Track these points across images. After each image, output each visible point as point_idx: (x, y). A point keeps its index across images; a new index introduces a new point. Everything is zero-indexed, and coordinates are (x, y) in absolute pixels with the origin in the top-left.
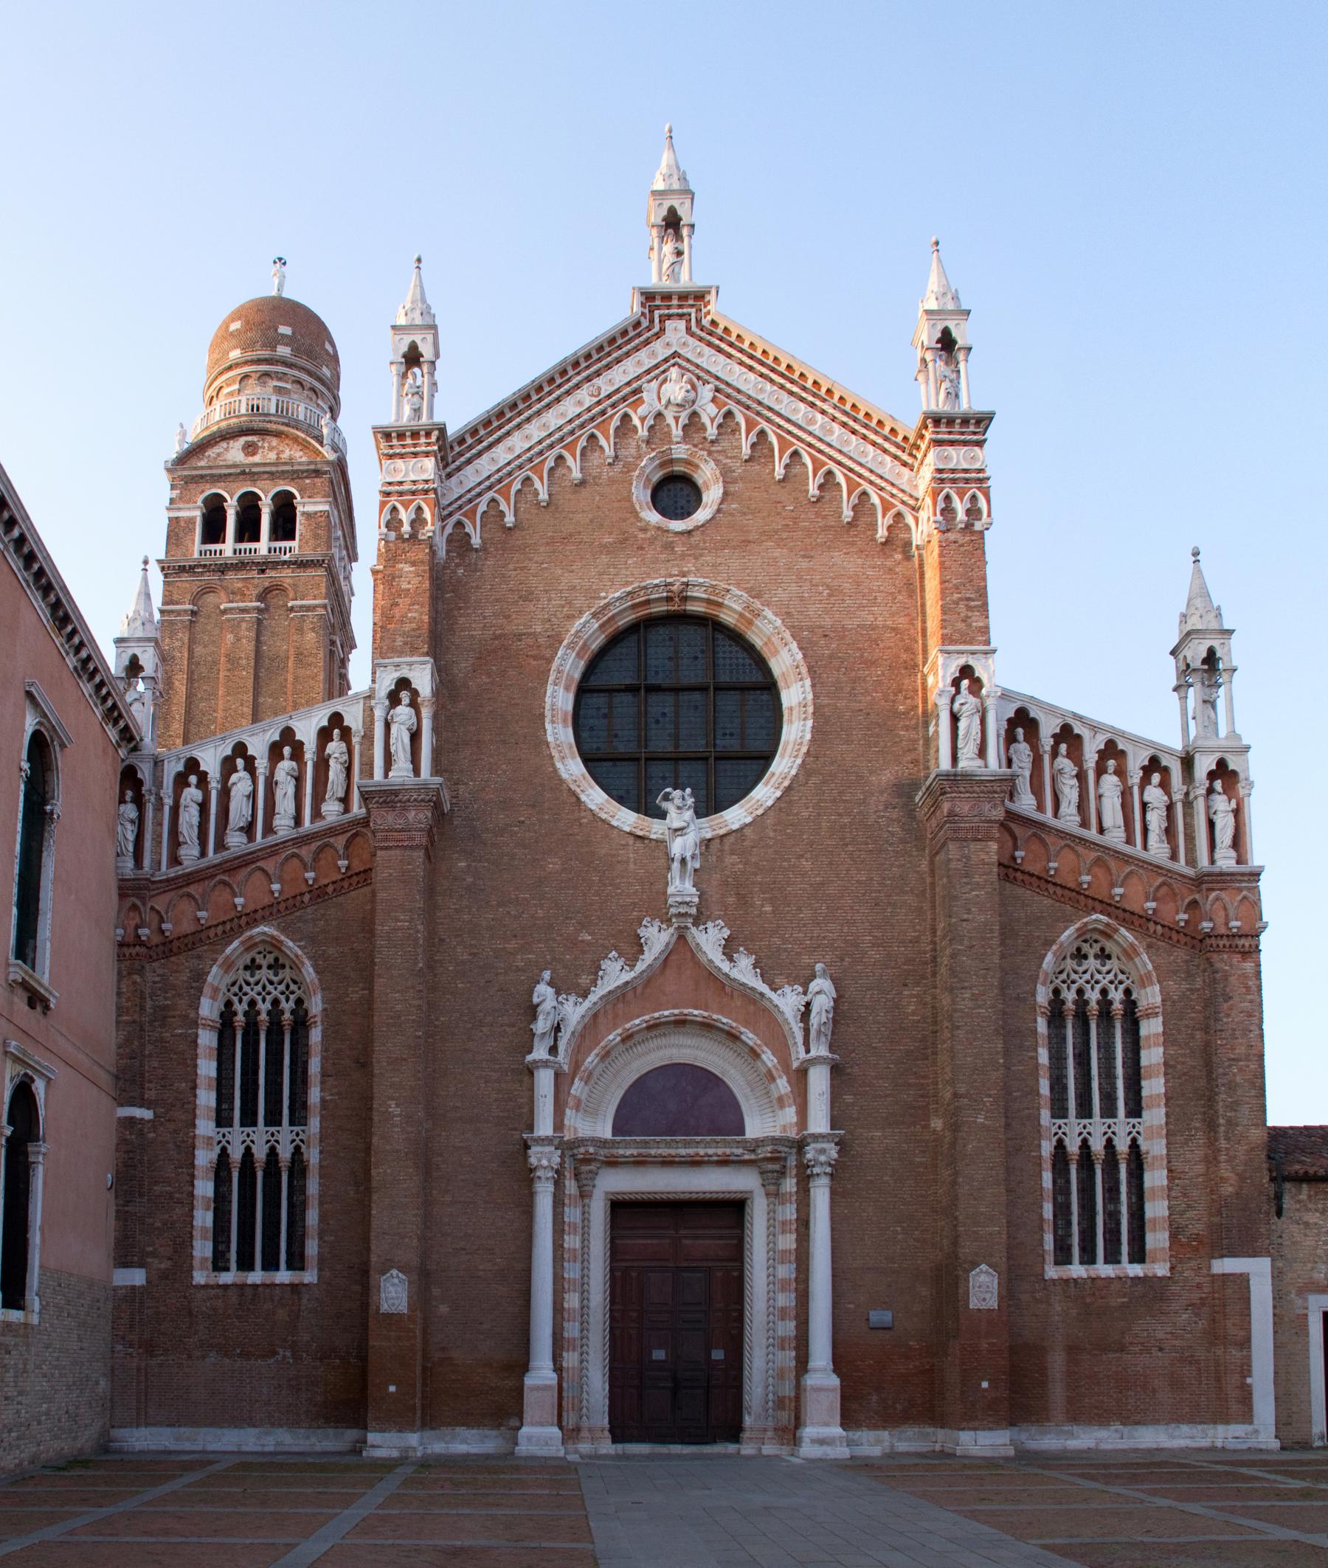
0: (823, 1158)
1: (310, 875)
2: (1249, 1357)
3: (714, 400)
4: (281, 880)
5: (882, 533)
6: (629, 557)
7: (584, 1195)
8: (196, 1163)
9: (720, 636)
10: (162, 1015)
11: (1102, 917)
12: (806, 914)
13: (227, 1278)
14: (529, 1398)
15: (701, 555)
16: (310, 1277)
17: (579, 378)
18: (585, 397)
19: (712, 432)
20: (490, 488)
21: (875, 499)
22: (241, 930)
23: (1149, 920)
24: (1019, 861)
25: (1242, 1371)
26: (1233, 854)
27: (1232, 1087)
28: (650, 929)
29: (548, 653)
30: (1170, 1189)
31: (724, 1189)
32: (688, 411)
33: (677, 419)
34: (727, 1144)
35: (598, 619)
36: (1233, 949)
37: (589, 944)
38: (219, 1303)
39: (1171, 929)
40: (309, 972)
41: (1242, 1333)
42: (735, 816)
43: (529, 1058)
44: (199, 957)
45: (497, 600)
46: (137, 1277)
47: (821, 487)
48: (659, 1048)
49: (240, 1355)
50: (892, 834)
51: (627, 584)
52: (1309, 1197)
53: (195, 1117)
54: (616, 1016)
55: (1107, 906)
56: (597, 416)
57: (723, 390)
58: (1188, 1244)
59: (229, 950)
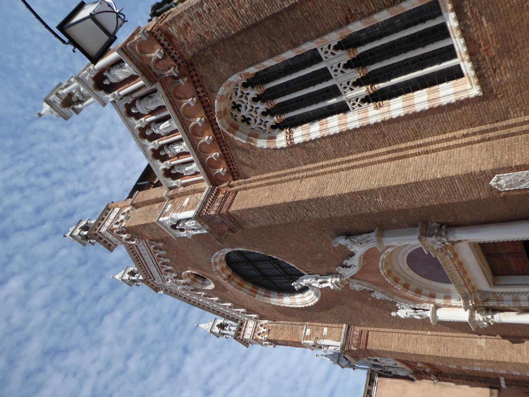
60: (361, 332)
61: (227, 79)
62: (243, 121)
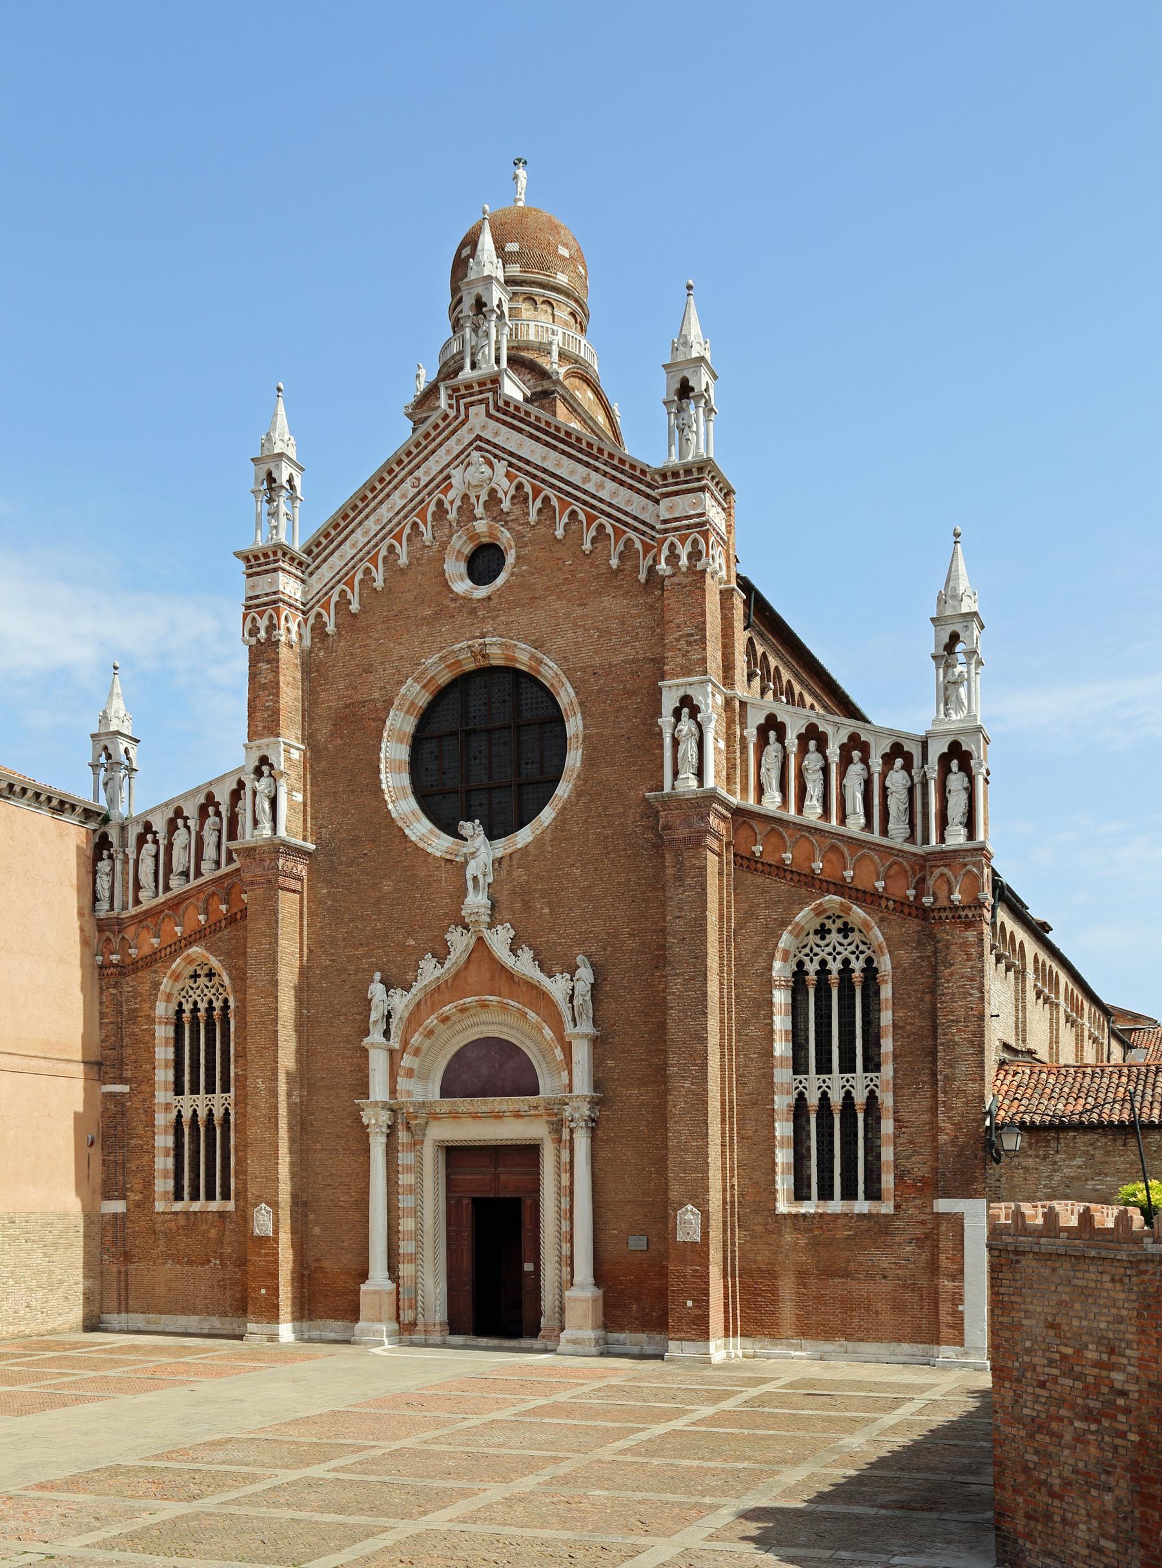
2: (961, 1288)
4: (206, 912)
5: (642, 577)
6: (443, 625)
7: (416, 1144)
10: (133, 1016)
11: (835, 897)
12: (576, 912)
13: (178, 1206)
15: (498, 616)
16: (230, 1206)
17: (403, 474)
19: (506, 505)
20: (339, 581)
27: (951, 1046)
29: (382, 715)
30: (896, 1137)
31: (520, 1137)
32: (487, 489)
33: (478, 497)
37: (414, 947)
38: (173, 1225)
42: (524, 836)
43: (366, 1041)
44: (156, 972)
45: (347, 675)
46: (117, 1207)
47: (594, 540)
49: (187, 1263)
50: (647, 840)
51: (442, 648)
55: (840, 888)
56: (416, 506)
58: (914, 1186)
59: (174, 966)
60: (299, 879)
61: (890, 952)
62: (823, 925)
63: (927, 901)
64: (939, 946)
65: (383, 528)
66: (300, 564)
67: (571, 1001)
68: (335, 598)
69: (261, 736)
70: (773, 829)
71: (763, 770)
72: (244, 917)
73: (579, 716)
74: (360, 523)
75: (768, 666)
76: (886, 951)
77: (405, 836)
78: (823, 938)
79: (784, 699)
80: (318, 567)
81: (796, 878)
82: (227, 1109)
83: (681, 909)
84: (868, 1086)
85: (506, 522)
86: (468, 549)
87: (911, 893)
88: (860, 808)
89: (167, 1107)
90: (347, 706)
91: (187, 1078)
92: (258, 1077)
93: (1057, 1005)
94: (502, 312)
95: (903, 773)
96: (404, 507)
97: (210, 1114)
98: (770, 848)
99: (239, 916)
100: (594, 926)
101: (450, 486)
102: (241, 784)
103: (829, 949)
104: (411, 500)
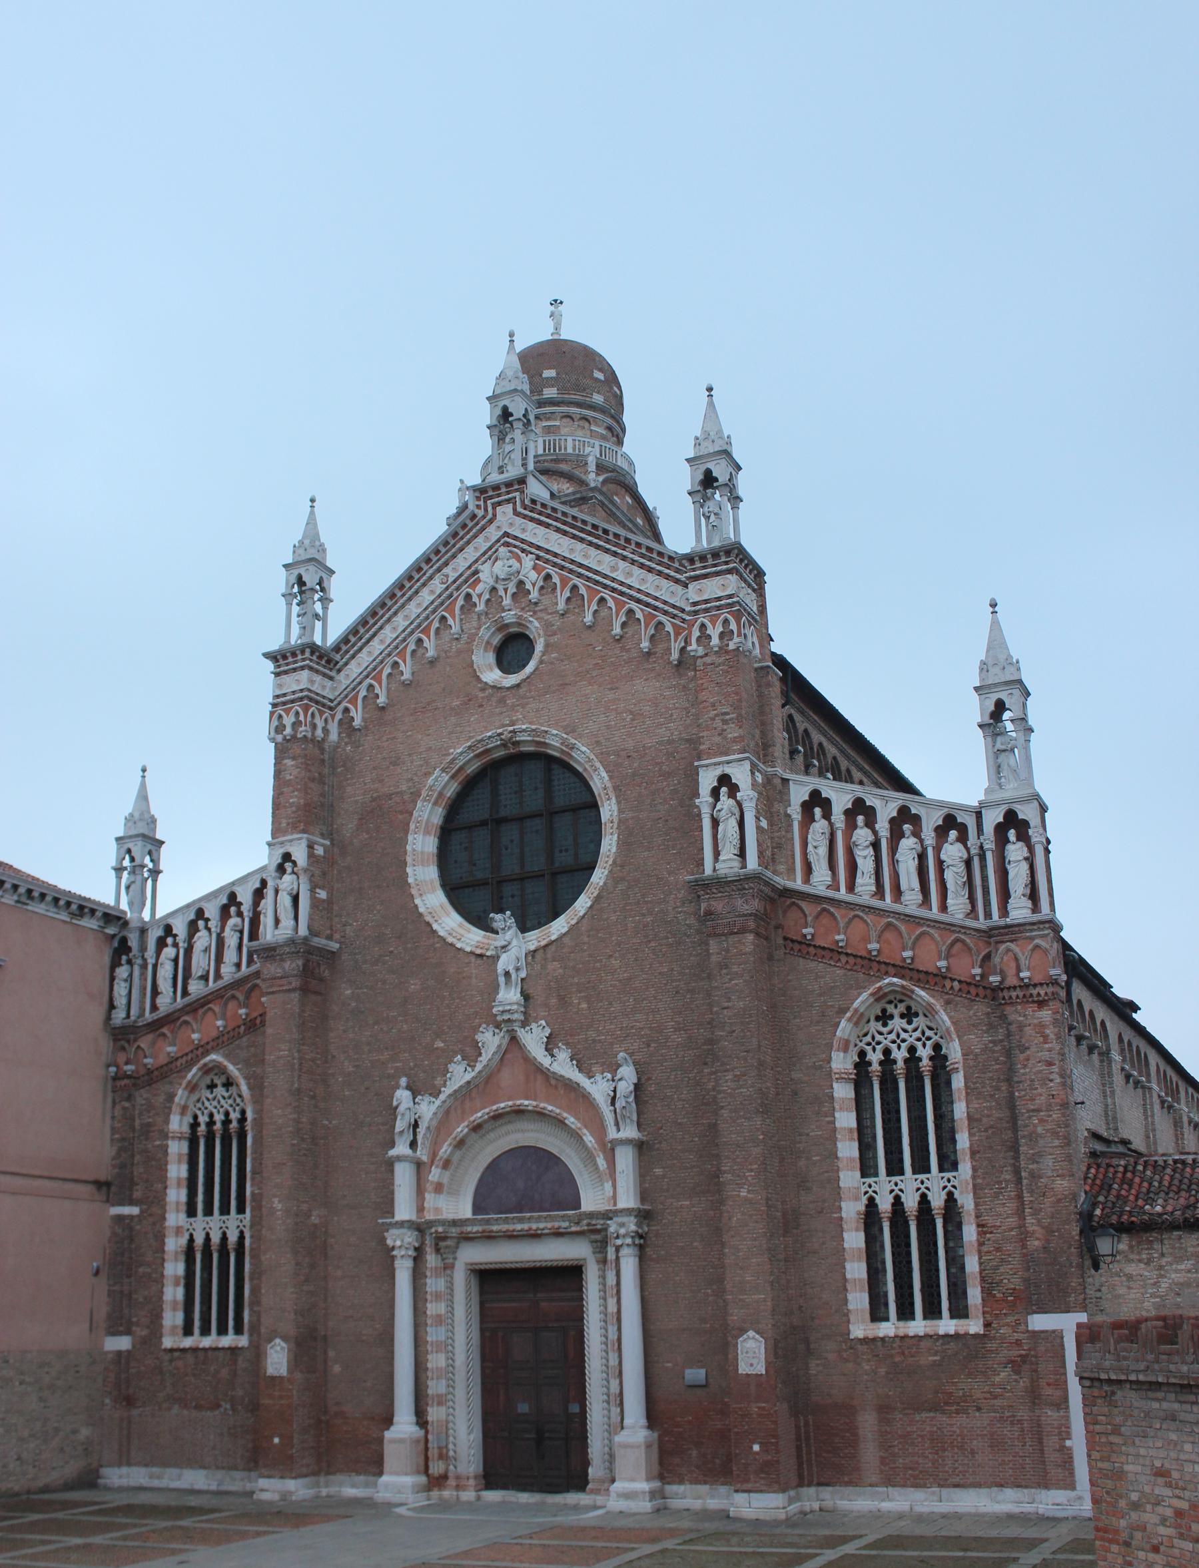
0: (622, 1231)
1: (242, 1011)
3: (535, 568)
5: (675, 655)
8: (166, 1249)
9: (555, 767)
11: (895, 980)
13: (188, 1342)
14: (388, 1449)
16: (243, 1341)
17: (431, 571)
18: (437, 585)
19: (534, 595)
20: (367, 677)
21: (669, 628)
22: (198, 1058)
23: (945, 978)
24: (809, 937)
25: (1060, 1434)
26: (1029, 904)
27: (1033, 1137)
28: (486, 1034)
30: (981, 1244)
32: (515, 581)
33: (506, 590)
34: (553, 1219)
35: (447, 773)
36: (1027, 1000)
37: (442, 1050)
39: (969, 984)
40: (244, 1088)
41: (1058, 1393)
42: (559, 926)
43: (392, 1153)
44: (171, 1083)
45: (374, 768)
46: (123, 1343)
47: (624, 625)
48: (508, 1133)
50: (689, 926)
52: (1131, 1247)
53: (165, 1212)
54: (463, 1112)
55: (901, 970)
56: (445, 601)
57: (543, 555)
59: (189, 1076)
62: (884, 1011)
63: (994, 979)
64: (1013, 1028)
65: (411, 623)
66: (329, 661)
67: (613, 1103)
68: (363, 693)
69: (285, 833)
70: (824, 910)
71: (810, 848)
72: (263, 1023)
73: (614, 800)
74: (389, 620)
75: (811, 743)
76: (954, 1036)
77: (435, 932)
78: (885, 1025)
79: (829, 775)
80: (346, 664)
81: (852, 960)
82: (242, 1232)
83: (729, 999)
84: (945, 1187)
85: (535, 612)
86: (496, 640)
87: (977, 971)
88: (916, 884)
89: (178, 1231)
90: (374, 800)
91: (200, 1198)
92: (275, 1196)
93: (1150, 1089)
94: (529, 420)
95: (959, 846)
96: (432, 603)
97: (224, 1238)
98: (822, 930)
99: (258, 1021)
100: (636, 1021)
101: (478, 581)
102: (264, 883)
103: (893, 1036)
104: (439, 596)
